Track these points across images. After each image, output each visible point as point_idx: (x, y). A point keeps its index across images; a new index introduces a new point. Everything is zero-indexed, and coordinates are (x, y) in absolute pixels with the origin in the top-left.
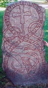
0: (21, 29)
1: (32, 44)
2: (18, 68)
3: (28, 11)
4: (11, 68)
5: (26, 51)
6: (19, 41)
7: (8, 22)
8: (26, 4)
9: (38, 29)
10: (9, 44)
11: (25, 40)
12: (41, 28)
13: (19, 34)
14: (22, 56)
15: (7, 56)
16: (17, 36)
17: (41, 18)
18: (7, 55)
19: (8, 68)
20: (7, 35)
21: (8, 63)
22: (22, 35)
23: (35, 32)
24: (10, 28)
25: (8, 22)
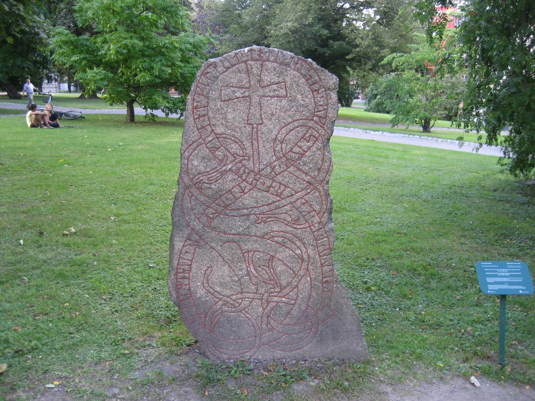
0: (247, 145)
2: (228, 292)
3: (277, 81)
4: (201, 292)
5: (262, 228)
8: (272, 58)
9: (309, 148)
10: (202, 198)
11: (259, 186)
12: (319, 144)
13: (241, 162)
14: (245, 248)
15: (188, 242)
16: (230, 169)
17: (321, 108)
18: (188, 239)
19: (189, 289)
20: (196, 163)
21: (194, 270)
22: (250, 165)
23: (299, 158)
24: (210, 139)
25: (204, 116)
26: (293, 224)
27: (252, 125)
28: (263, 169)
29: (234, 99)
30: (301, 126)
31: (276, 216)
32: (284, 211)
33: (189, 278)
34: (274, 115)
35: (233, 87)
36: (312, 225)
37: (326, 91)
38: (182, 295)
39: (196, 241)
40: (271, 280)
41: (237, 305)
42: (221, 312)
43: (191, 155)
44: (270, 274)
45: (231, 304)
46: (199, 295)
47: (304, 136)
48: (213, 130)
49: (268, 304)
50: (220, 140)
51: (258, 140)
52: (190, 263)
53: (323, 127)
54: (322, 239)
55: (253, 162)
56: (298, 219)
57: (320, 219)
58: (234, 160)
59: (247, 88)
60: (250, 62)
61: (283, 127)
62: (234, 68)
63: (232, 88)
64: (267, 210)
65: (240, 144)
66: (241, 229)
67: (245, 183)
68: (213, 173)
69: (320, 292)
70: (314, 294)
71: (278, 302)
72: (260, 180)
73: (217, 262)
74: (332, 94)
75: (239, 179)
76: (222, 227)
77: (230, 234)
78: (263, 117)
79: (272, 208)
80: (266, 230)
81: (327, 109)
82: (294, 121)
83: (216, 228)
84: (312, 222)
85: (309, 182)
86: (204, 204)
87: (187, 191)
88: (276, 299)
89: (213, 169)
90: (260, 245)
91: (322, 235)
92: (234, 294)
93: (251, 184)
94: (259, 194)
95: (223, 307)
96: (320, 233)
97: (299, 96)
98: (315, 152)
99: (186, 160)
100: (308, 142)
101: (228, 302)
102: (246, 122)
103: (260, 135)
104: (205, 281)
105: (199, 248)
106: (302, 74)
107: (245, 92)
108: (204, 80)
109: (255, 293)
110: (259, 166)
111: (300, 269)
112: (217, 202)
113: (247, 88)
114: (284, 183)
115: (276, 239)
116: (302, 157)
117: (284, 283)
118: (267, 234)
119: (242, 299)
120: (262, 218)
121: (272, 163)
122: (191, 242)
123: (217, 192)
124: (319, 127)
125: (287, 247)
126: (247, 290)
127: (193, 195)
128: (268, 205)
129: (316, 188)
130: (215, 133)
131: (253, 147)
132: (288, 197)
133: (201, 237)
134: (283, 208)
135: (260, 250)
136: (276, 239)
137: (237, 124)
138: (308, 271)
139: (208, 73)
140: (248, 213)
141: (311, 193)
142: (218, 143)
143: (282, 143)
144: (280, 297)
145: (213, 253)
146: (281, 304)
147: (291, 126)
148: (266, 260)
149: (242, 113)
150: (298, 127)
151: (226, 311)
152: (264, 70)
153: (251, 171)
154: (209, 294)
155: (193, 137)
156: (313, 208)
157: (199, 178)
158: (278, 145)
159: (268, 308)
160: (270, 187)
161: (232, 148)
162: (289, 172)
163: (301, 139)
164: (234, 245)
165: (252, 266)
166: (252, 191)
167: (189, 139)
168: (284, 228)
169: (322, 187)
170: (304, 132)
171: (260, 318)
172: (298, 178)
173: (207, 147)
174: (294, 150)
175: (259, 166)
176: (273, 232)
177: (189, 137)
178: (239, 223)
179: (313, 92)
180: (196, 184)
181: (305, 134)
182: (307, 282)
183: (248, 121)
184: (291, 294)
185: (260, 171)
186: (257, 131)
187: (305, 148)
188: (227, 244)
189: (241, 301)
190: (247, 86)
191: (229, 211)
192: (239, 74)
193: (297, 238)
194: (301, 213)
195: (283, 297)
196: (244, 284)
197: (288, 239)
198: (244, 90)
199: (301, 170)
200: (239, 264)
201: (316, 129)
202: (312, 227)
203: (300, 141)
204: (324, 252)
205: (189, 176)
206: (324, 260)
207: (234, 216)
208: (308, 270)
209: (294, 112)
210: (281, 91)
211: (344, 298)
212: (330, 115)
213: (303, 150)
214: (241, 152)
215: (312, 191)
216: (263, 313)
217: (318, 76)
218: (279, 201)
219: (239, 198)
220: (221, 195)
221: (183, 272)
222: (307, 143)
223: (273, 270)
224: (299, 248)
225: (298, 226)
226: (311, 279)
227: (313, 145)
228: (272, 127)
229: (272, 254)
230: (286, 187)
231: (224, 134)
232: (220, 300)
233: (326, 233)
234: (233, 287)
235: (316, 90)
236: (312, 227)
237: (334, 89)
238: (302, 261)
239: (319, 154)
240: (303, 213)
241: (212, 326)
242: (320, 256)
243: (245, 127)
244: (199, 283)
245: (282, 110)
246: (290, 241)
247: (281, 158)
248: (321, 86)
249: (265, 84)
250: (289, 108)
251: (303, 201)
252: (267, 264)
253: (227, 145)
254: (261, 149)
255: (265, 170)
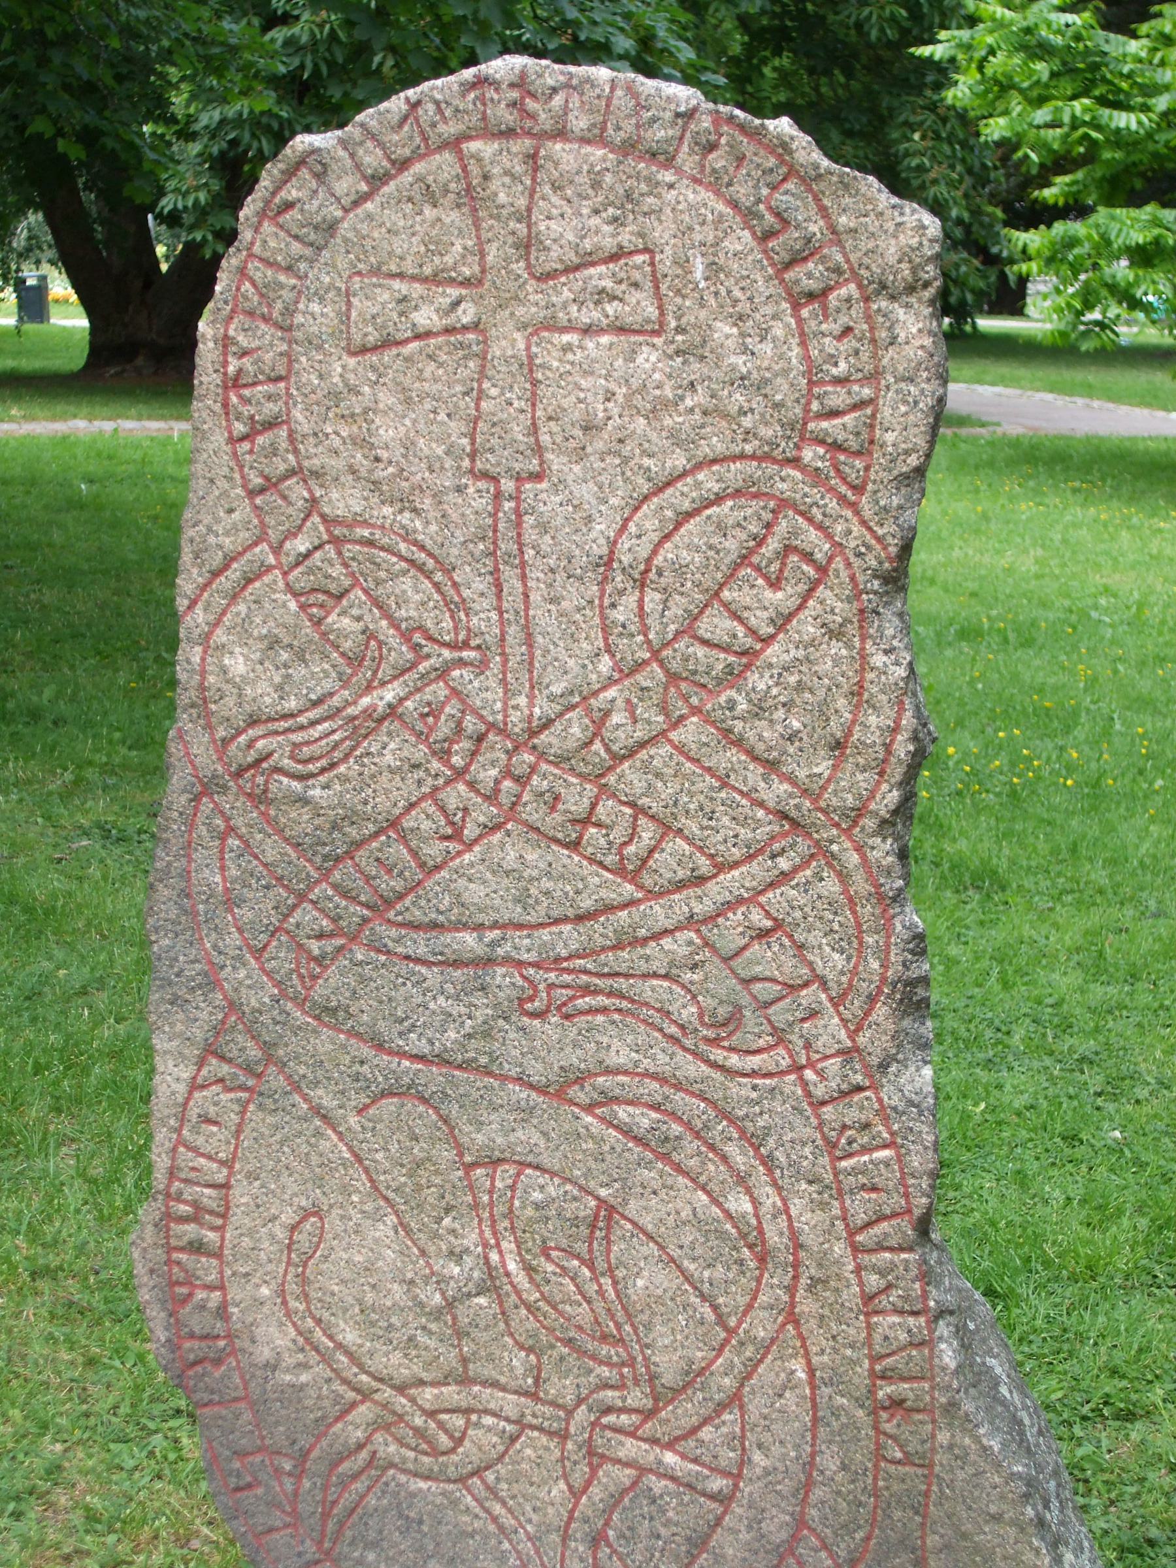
0: (475, 585)
1: (658, 913)
2: (393, 1362)
3: (609, 244)
6: (423, 821)
7: (271, 425)
8: (579, 123)
9: (783, 621)
10: (272, 849)
11: (532, 812)
13: (442, 673)
15: (215, 1067)
16: (392, 711)
17: (838, 398)
18: (211, 1051)
19: (222, 1312)
20: (237, 665)
21: (238, 1217)
23: (733, 677)
24: (301, 545)
25: (271, 425)
26: (708, 1041)
27: (495, 479)
28: (547, 724)
29: (406, 341)
30: (738, 493)
31: (622, 984)
32: (655, 966)
33: (218, 1255)
34: (599, 429)
35: (401, 276)
36: (811, 1064)
37: (867, 299)
38: (192, 1336)
39: (249, 1070)
40: (604, 1338)
41: (444, 1441)
42: (370, 1464)
43: (217, 623)
44: (599, 1305)
45: (416, 1430)
46: (264, 1353)
47: (752, 551)
48: (313, 501)
49: (594, 1470)
50: (350, 550)
51: (523, 564)
52: (221, 1176)
53: (854, 506)
54: (865, 1150)
55: (504, 682)
56: (734, 1020)
57: (852, 1035)
58: (414, 665)
59: (466, 283)
60: (474, 146)
61: (646, 498)
62: (407, 178)
63: (396, 284)
64: (574, 946)
65: (438, 577)
66: (452, 1035)
67: (461, 787)
68: (313, 723)
69: (861, 1457)
70: (829, 1462)
71: (643, 1470)
72: (535, 779)
73: (346, 1190)
74: (901, 313)
75: (435, 765)
76: (365, 1013)
77: (402, 1054)
78: (545, 439)
79: (600, 941)
80: (573, 1058)
81: (871, 401)
82: (699, 466)
83: (335, 1010)
84: (808, 1046)
85: (784, 815)
86: (280, 879)
87: (206, 805)
88: (630, 1448)
89: (316, 704)
90: (545, 1134)
91: (866, 1126)
92: (425, 1376)
93: (492, 797)
94: (531, 856)
95: (379, 1437)
96: (852, 1115)
97: (724, 330)
98: (812, 643)
99: (198, 649)
100: (775, 584)
101: (401, 1417)
102: (466, 463)
103: (530, 535)
104: (292, 1287)
105: (261, 1107)
106: (734, 204)
107: (456, 303)
108: (272, 244)
109: (526, 1394)
110: (531, 705)
111: (749, 1307)
112: (337, 876)
113: (466, 283)
114: (655, 808)
115: (623, 1113)
116: (748, 666)
117: (668, 1367)
118: (579, 1081)
119: (467, 1411)
120: (551, 987)
121: (595, 694)
122: (225, 1069)
123: (335, 826)
124: (833, 505)
125: (679, 1169)
126: (488, 1371)
127: (231, 830)
128: (580, 918)
129: (821, 852)
130: (323, 517)
131: (499, 597)
132: (680, 885)
133: (267, 1048)
134: (651, 949)
135: (546, 1161)
136: (623, 1113)
137: (420, 473)
138: (797, 1323)
139: (289, 206)
140: (480, 950)
141: (800, 878)
142: (337, 571)
143: (642, 584)
144: (654, 1441)
145: (324, 1145)
146: (658, 1485)
147: (680, 497)
148: (575, 1221)
149: (442, 417)
150: (719, 499)
151: (392, 1465)
152: (547, 189)
153: (491, 726)
154: (314, 1357)
155: (227, 533)
156: (810, 965)
157: (250, 745)
158: (622, 593)
159: (595, 1491)
160: (586, 821)
161: (402, 601)
162: (680, 749)
163: (736, 567)
164: (423, 1117)
165: (508, 1245)
166: (497, 837)
167: (212, 540)
168: (662, 1058)
169: (859, 849)
170: (754, 528)
171: (555, 1537)
172: (725, 785)
173: (289, 588)
174: (704, 628)
175: (531, 705)
176: (608, 1071)
177: (210, 529)
178: (441, 1000)
179: (796, 307)
180: (239, 774)
181: (761, 541)
182: (790, 1383)
183: (473, 456)
184: (706, 1433)
185: (533, 733)
186: (519, 516)
187: (760, 620)
188: (390, 1104)
189: (459, 1421)
190: (467, 272)
191: (394, 933)
192: (429, 212)
193: (731, 1122)
194: (747, 982)
195: (670, 1446)
196: (475, 1333)
197: (688, 1126)
198: (454, 292)
199: (739, 743)
200: (447, 1221)
201: (816, 512)
202: (809, 1074)
203: (730, 576)
204: (877, 1230)
205: (209, 727)
206: (882, 1273)
207: (418, 961)
208: (793, 1318)
209: (697, 417)
210: (634, 297)
211: (997, 1518)
212: (890, 437)
213: (752, 632)
214: (447, 624)
215: (806, 864)
216: (571, 1518)
217: (823, 211)
218: (632, 903)
219: (438, 868)
220: (359, 844)
221: (194, 1219)
222: (768, 594)
223: (615, 1283)
224: (742, 1180)
225: (734, 1060)
226: (811, 1372)
227: (800, 607)
228: (586, 492)
229: (603, 1192)
230: (667, 829)
231: (365, 523)
232: (366, 1395)
233: (886, 1120)
234: (422, 1338)
235: (811, 296)
236: (809, 1074)
237: (911, 289)
238: (762, 1260)
239: (837, 661)
240: (757, 987)
241: (331, 1526)
242: (856, 1249)
243: (459, 489)
244: (265, 1291)
245: (638, 400)
246: (697, 1135)
247: (640, 665)
248: (838, 270)
249: (553, 258)
250: (668, 393)
251: (758, 918)
252: (581, 1247)
253: (378, 583)
254: (543, 617)
255: (558, 726)
